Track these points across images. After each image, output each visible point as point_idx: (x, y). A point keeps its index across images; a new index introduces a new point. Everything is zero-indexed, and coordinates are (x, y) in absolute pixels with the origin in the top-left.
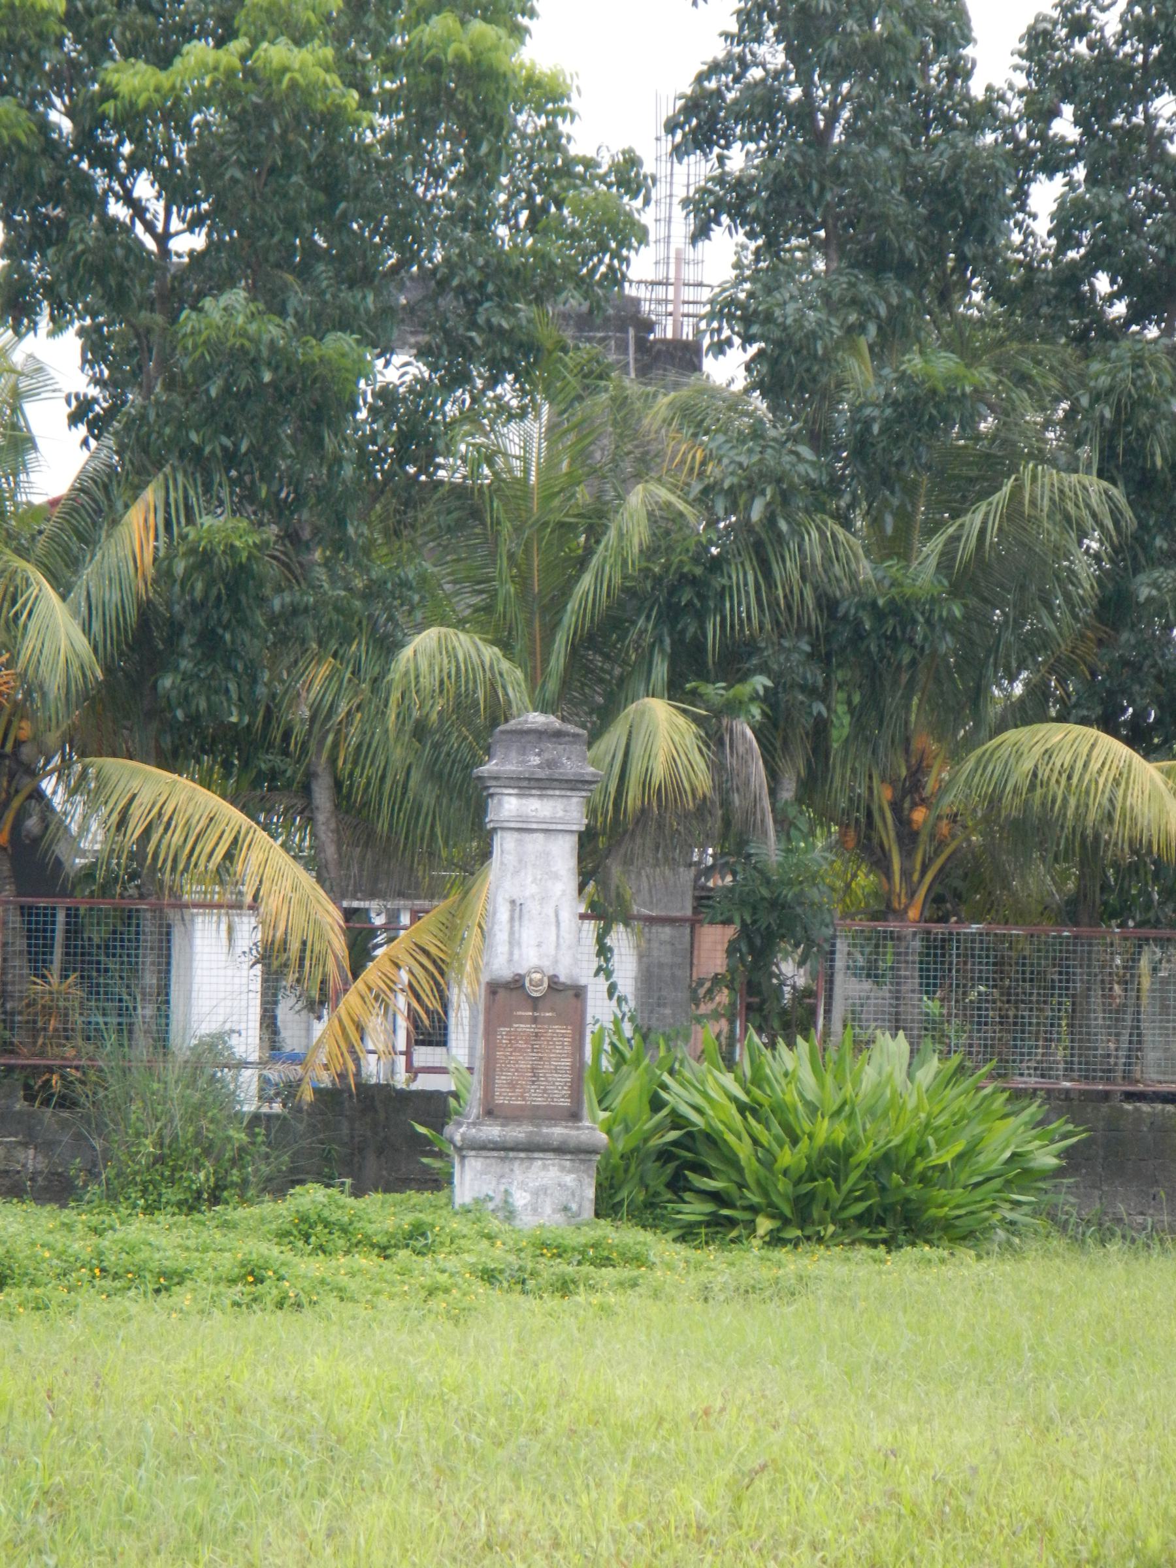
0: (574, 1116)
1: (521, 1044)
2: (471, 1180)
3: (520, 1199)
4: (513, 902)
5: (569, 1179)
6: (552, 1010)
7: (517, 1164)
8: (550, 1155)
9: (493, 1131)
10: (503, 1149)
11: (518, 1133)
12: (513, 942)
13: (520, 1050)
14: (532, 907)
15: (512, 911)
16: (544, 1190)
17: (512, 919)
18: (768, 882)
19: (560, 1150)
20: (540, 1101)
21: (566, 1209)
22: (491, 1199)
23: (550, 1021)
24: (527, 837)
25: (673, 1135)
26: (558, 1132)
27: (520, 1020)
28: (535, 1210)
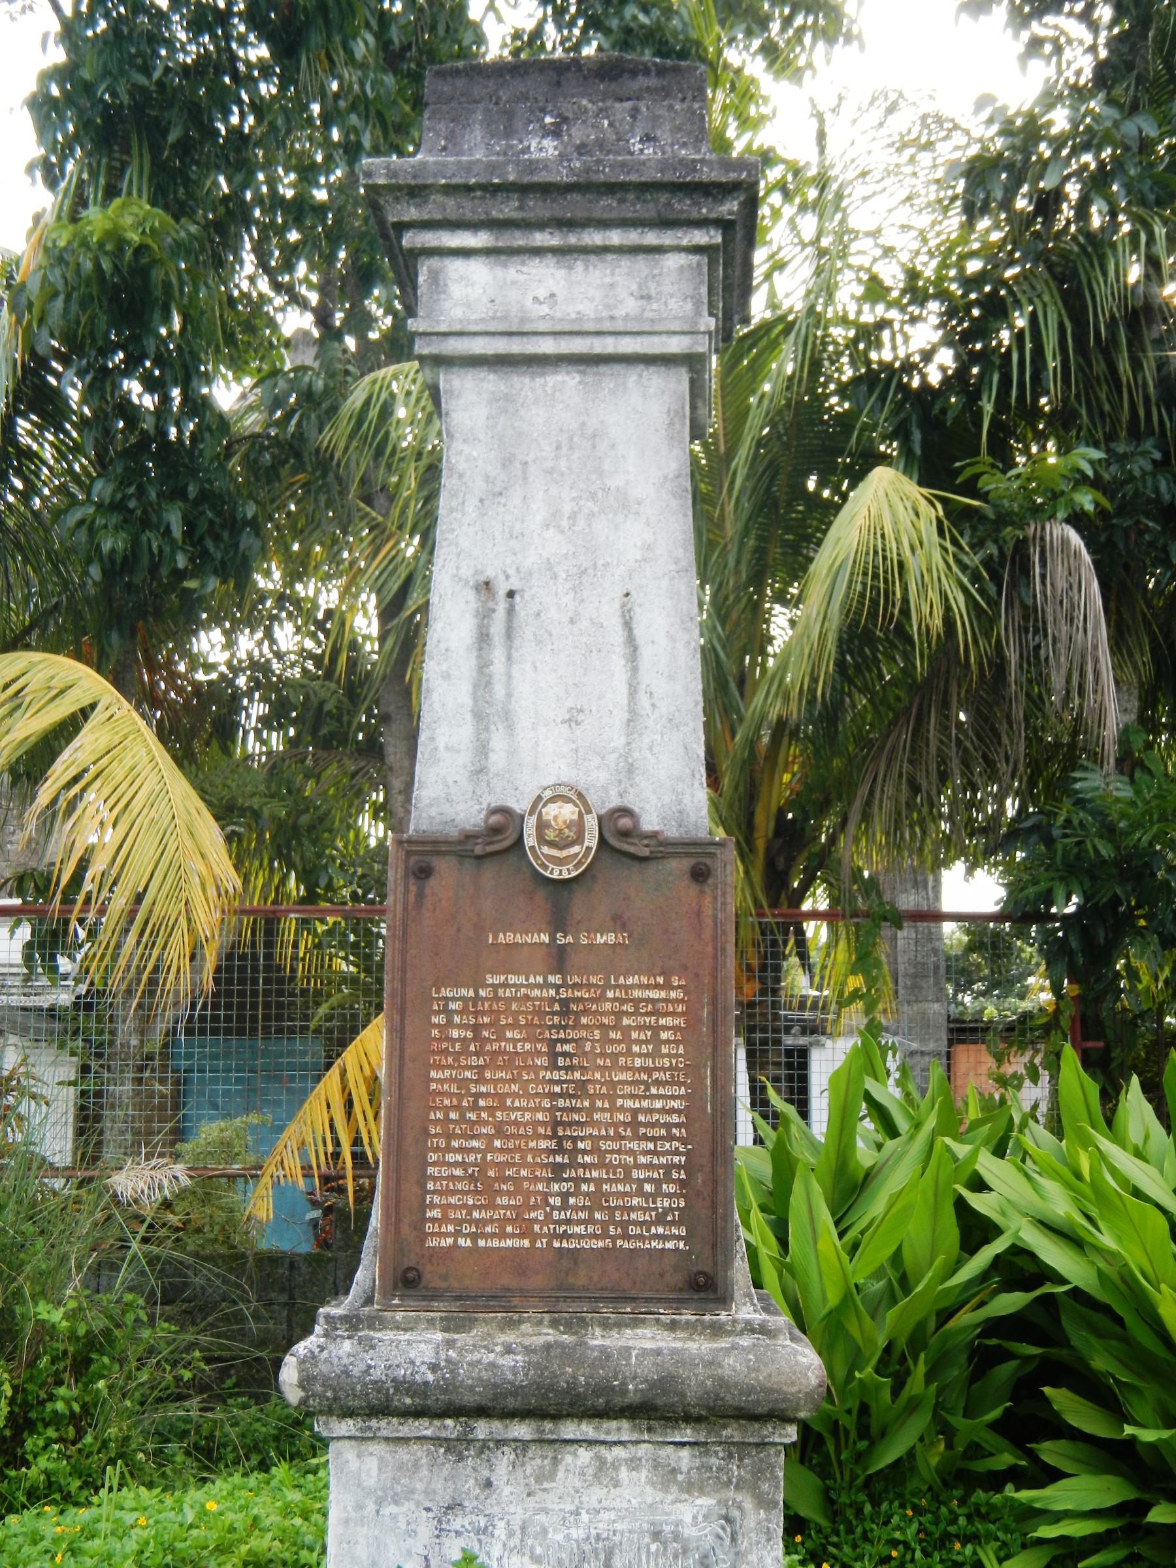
0: (703, 1288)
1: (515, 1040)
4: (487, 585)
5: (691, 1514)
6: (618, 922)
7: (503, 1461)
8: (622, 1429)
9: (414, 1348)
10: (451, 1412)
11: (500, 1351)
12: (487, 711)
13: (510, 1061)
14: (546, 601)
15: (485, 615)
17: (483, 638)
19: (654, 1409)
20: (584, 1237)
23: (611, 962)
24: (524, 384)
25: (1010, 1302)
26: (643, 1346)
27: (509, 959)
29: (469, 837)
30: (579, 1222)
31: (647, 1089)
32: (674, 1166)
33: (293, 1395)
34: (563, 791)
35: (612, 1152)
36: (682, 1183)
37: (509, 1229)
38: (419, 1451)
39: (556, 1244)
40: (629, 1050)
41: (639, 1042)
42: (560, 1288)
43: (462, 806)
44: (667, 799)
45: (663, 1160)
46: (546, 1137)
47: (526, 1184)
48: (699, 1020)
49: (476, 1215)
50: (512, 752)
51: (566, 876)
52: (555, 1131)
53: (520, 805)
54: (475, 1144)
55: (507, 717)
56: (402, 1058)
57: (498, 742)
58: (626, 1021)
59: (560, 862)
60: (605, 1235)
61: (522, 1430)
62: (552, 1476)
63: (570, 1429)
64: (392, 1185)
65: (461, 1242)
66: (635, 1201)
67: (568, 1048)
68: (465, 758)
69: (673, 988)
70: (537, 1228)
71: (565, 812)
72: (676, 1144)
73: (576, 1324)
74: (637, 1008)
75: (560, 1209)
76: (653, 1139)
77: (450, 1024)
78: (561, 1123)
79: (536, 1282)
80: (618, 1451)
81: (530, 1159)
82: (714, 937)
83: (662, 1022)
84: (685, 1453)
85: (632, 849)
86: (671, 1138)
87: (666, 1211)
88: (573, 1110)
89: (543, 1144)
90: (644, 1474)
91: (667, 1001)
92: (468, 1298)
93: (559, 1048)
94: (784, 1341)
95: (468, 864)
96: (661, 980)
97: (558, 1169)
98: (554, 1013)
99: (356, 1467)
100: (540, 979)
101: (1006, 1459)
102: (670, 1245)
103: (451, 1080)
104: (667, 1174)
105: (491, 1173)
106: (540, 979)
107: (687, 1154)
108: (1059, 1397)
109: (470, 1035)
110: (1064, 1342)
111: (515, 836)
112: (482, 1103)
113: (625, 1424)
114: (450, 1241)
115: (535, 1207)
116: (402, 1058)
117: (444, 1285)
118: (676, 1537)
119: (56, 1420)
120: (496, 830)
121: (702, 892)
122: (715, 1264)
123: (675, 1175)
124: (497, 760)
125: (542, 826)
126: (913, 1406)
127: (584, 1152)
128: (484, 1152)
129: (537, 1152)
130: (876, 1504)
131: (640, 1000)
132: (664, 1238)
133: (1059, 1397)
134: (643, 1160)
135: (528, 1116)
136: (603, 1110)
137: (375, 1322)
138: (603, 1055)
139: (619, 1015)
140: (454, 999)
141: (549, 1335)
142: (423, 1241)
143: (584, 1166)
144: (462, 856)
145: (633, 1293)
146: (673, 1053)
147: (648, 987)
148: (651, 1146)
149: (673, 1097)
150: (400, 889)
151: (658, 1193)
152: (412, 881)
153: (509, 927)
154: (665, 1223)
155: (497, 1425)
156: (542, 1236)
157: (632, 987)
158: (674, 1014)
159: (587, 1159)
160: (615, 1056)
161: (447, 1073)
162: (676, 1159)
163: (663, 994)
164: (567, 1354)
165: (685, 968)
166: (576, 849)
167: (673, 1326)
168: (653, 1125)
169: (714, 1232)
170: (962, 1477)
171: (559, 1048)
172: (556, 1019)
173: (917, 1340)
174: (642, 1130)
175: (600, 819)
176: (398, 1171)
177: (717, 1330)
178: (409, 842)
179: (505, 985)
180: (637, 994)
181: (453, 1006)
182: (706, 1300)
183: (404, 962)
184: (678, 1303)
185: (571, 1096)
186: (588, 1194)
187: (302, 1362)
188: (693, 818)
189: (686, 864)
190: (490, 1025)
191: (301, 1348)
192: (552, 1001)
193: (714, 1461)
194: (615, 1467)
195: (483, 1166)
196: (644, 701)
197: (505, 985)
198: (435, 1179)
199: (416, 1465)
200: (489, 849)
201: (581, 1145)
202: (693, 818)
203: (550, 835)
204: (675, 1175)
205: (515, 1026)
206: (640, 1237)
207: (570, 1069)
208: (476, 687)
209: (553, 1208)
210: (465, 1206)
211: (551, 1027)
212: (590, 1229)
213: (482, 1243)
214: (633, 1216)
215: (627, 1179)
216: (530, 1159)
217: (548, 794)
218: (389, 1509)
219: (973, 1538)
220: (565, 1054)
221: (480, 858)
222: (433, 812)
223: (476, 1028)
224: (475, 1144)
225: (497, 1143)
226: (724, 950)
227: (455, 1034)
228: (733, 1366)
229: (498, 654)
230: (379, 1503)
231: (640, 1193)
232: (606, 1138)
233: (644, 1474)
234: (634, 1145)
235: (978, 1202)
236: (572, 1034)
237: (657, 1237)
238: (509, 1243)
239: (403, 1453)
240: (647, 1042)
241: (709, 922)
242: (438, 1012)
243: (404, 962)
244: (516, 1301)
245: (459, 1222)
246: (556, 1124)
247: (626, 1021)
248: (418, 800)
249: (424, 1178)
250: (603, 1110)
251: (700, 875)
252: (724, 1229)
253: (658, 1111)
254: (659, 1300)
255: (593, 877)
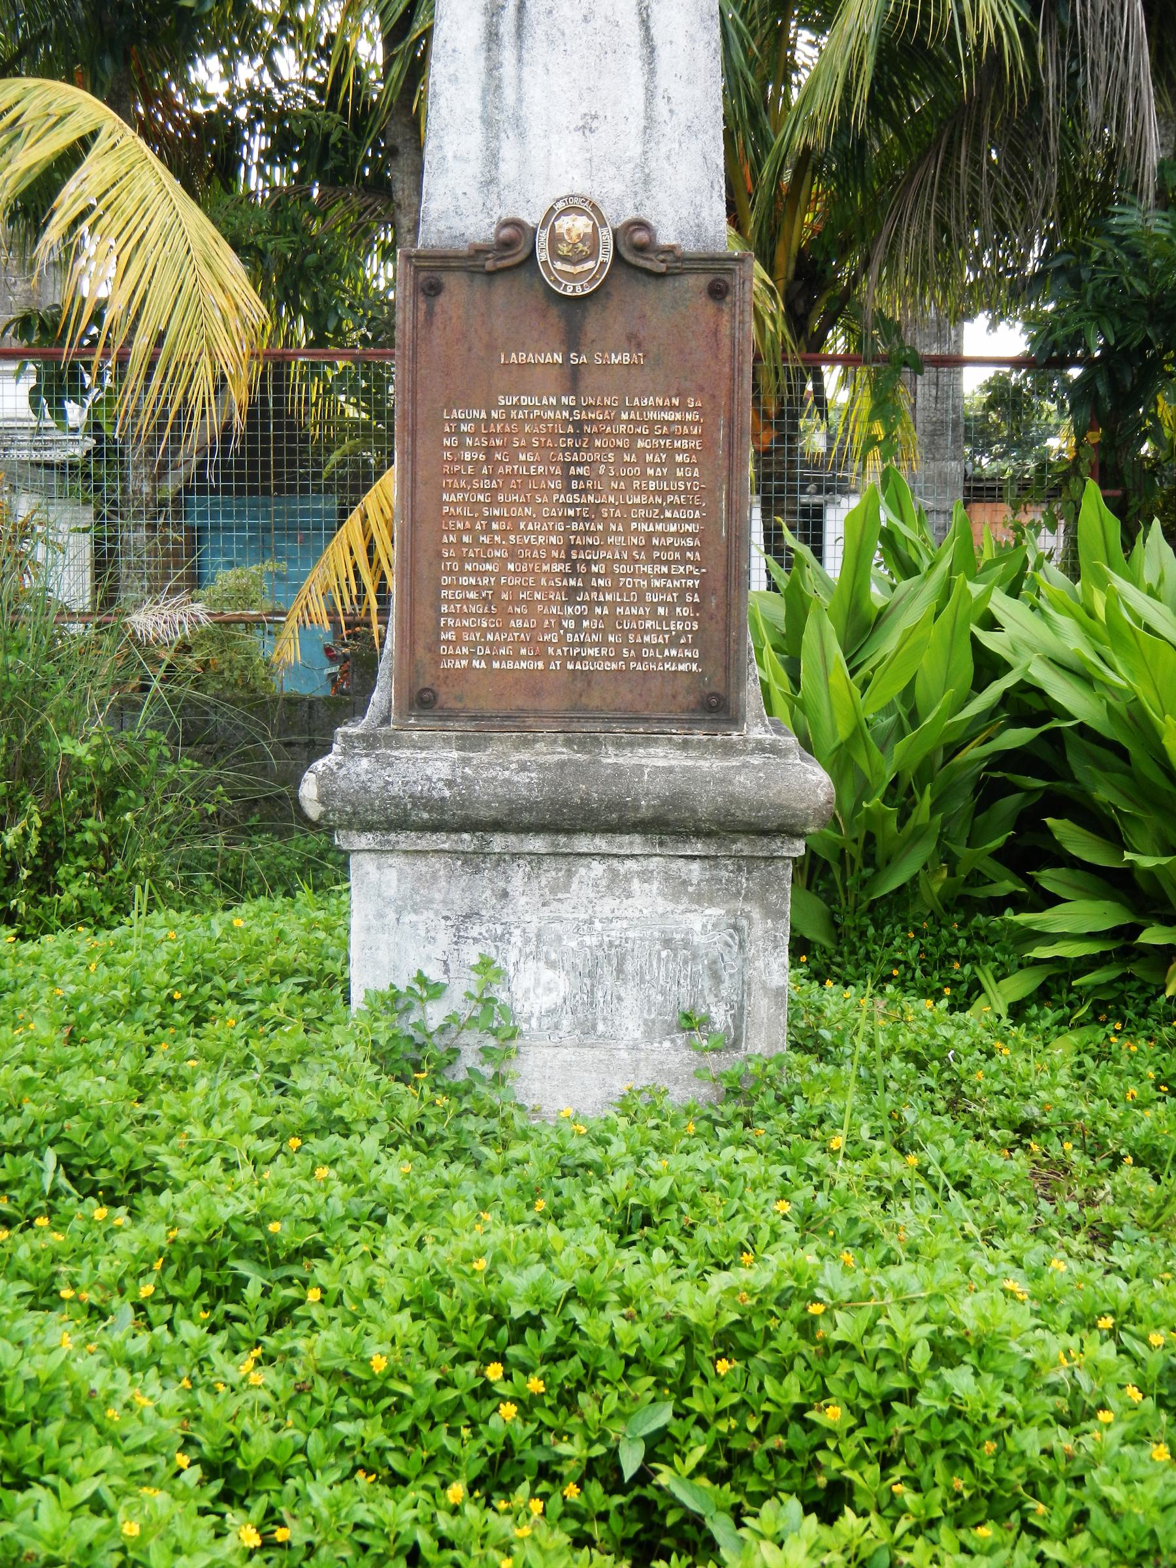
0: (715, 709)
2: (392, 925)
3: (536, 990)
5: (701, 923)
6: (634, 341)
7: (518, 875)
8: (635, 843)
9: (430, 765)
10: (467, 826)
11: (514, 768)
13: (523, 483)
16: (617, 958)
17: (492, 37)
18: (1142, 269)
19: (666, 824)
20: (598, 659)
21: (689, 1022)
22: (436, 991)
25: (1016, 737)
26: (657, 764)
28: (588, 1029)
29: (479, 252)
30: (593, 645)
31: (662, 512)
32: (688, 589)
33: (313, 810)
34: (576, 202)
35: (626, 575)
36: (696, 607)
37: (523, 651)
38: (436, 863)
39: (570, 667)
40: (644, 473)
41: (655, 465)
42: (574, 709)
43: (472, 220)
44: (684, 213)
45: (677, 583)
46: (559, 560)
47: (540, 608)
48: (715, 442)
49: (490, 637)
50: (523, 162)
51: (580, 293)
52: (568, 555)
53: (532, 217)
54: (489, 567)
55: (517, 121)
56: (414, 481)
57: (508, 150)
58: (640, 444)
59: (573, 277)
60: (618, 657)
61: (537, 844)
62: (566, 887)
63: (583, 843)
64: (407, 607)
65: (476, 663)
66: (649, 624)
67: (581, 471)
68: (475, 168)
69: (689, 410)
70: (551, 650)
71: (579, 225)
72: (690, 567)
73: (589, 743)
74: (652, 430)
75: (574, 632)
76: (667, 562)
77: (462, 446)
78: (575, 546)
79: (548, 703)
80: (630, 864)
81: (543, 582)
82: (732, 357)
83: (677, 444)
84: (695, 866)
85: (648, 265)
86: (688, 562)
87: (679, 634)
88: (587, 533)
89: (557, 568)
90: (655, 885)
91: (682, 422)
92: (483, 718)
93: (572, 471)
94: (794, 759)
95: (479, 280)
96: (676, 401)
97: (572, 592)
98: (567, 435)
99: (377, 880)
100: (553, 401)
101: (1007, 886)
102: (683, 667)
103: (464, 503)
104: (681, 597)
105: (505, 596)
106: (553, 401)
107: (702, 577)
108: (1060, 827)
109: (482, 457)
110: (1070, 777)
111: (527, 251)
112: (495, 526)
113: (638, 838)
114: (464, 663)
115: (549, 630)
116: (414, 481)
117: (459, 705)
118: (686, 944)
119: (85, 849)
120: (506, 245)
121: (720, 310)
122: (727, 686)
123: (689, 599)
124: (508, 170)
125: (555, 239)
126: (919, 835)
127: (598, 575)
128: (497, 576)
129: (550, 575)
130: (879, 926)
131: (656, 422)
132: (677, 660)
133: (1060, 827)
134: (657, 583)
135: (541, 539)
136: (617, 533)
137: (392, 741)
138: (617, 478)
139: (634, 437)
140: (465, 421)
141: (563, 753)
142: (438, 663)
143: (598, 589)
144: (472, 272)
145: (646, 714)
146: (687, 476)
147: (663, 408)
148: (665, 569)
149: (688, 521)
150: (410, 306)
151: (672, 616)
152: (421, 298)
153: (522, 347)
154: (678, 646)
155: (512, 839)
156: (555, 658)
157: (646, 408)
158: (689, 436)
159: (601, 582)
160: (629, 479)
161: (460, 496)
162: (690, 583)
163: (678, 416)
164: (580, 770)
165: (702, 389)
166: (590, 264)
167: (685, 745)
168: (667, 548)
169: (727, 653)
170: (962, 903)
171: (572, 471)
172: (570, 442)
173: (924, 773)
174: (656, 554)
175: (615, 233)
176: (411, 594)
177: (728, 750)
178: (418, 257)
179: (518, 407)
180: (652, 415)
181: (464, 428)
182: (717, 721)
183: (414, 383)
184: (691, 723)
185: (585, 520)
186: (601, 617)
187: (321, 778)
188: (711, 232)
189: (703, 280)
190: (503, 447)
191: (319, 765)
192: (566, 422)
193: (724, 874)
194: (627, 879)
195: (497, 590)
196: (661, 107)
197: (518, 407)
198: (449, 602)
199: (435, 876)
200: (500, 264)
201: (594, 569)
202: (711, 232)
203: (564, 249)
204: (689, 599)
205: (528, 448)
206: (654, 659)
207: (583, 492)
208: (485, 91)
209: (567, 631)
210: (479, 628)
211: (566, 449)
212: (604, 652)
213: (496, 665)
214: (647, 639)
215: (641, 601)
216: (543, 582)
217: (561, 206)
218: (408, 918)
219: (972, 959)
220: (579, 477)
221: (490, 274)
222: (442, 226)
223: (489, 450)
224: (489, 567)
225: (511, 567)
226: (741, 370)
227: (467, 456)
228: (744, 783)
229: (508, 55)
230: (399, 911)
231: (654, 616)
232: (621, 561)
233: (655, 885)
234: (648, 569)
235: (989, 640)
236: (586, 457)
237: (670, 659)
238: (524, 665)
239: (421, 866)
240: (661, 465)
241: (726, 341)
242: (450, 434)
243: (414, 383)
244: (530, 721)
245: (474, 644)
246: (570, 547)
247: (640, 444)
248: (427, 213)
249: (438, 601)
250: (617, 533)
251: (718, 292)
252: (737, 651)
253: (672, 534)
254: (671, 721)
255: (608, 295)
